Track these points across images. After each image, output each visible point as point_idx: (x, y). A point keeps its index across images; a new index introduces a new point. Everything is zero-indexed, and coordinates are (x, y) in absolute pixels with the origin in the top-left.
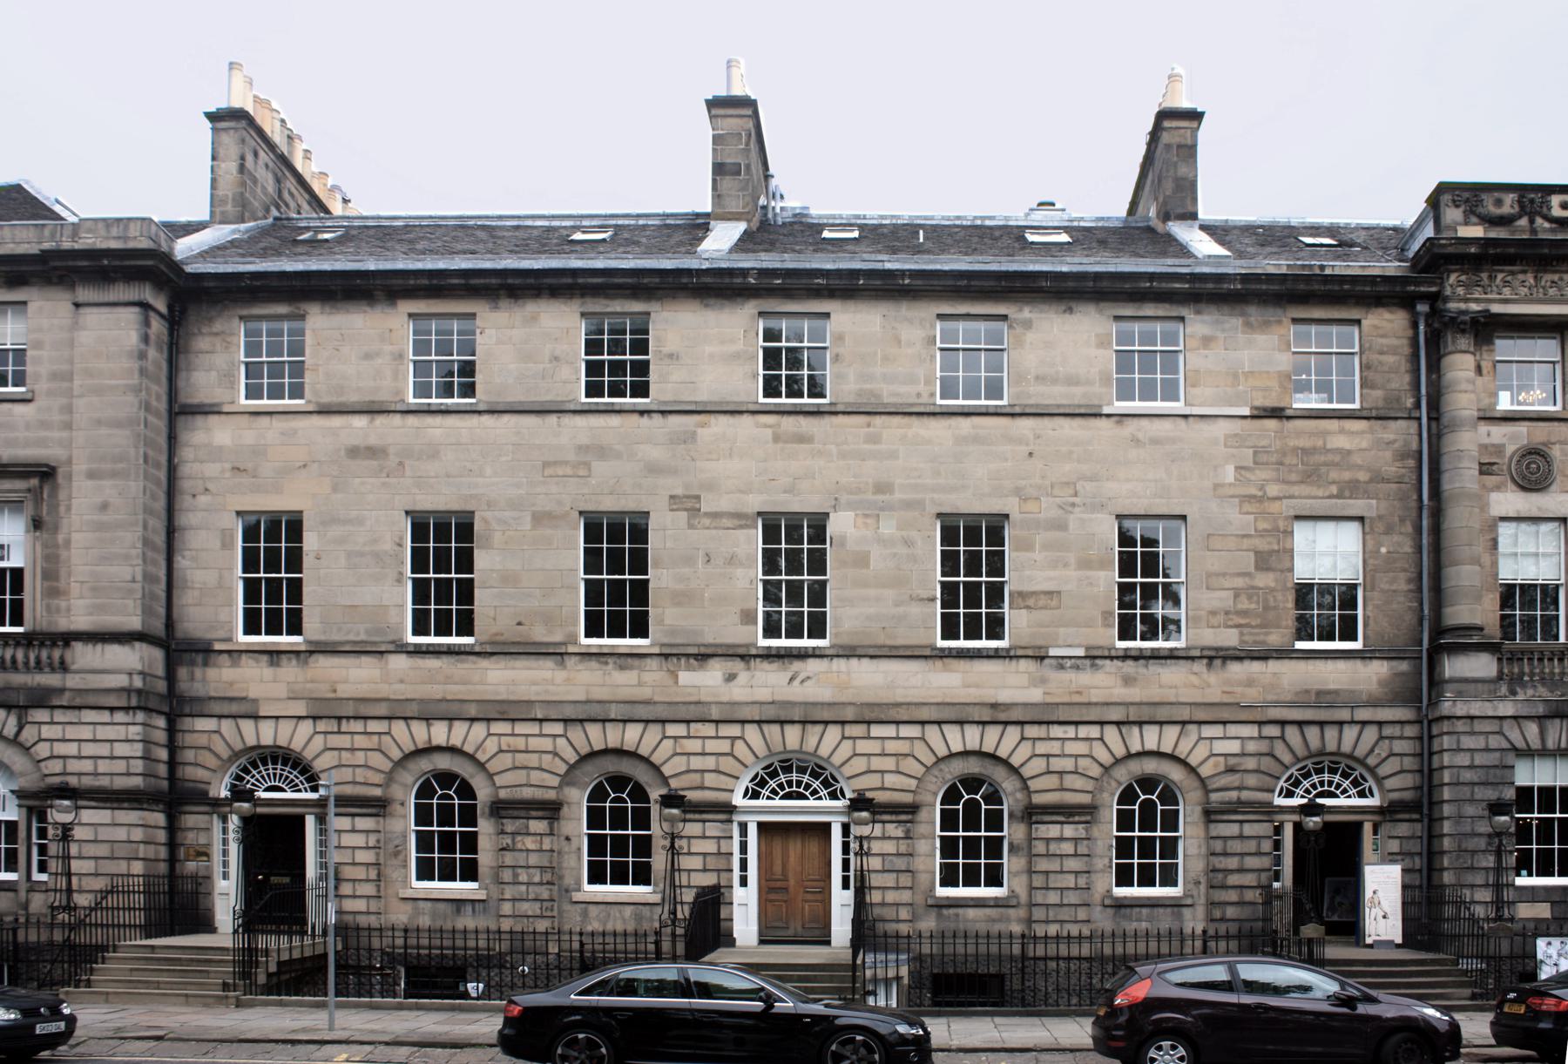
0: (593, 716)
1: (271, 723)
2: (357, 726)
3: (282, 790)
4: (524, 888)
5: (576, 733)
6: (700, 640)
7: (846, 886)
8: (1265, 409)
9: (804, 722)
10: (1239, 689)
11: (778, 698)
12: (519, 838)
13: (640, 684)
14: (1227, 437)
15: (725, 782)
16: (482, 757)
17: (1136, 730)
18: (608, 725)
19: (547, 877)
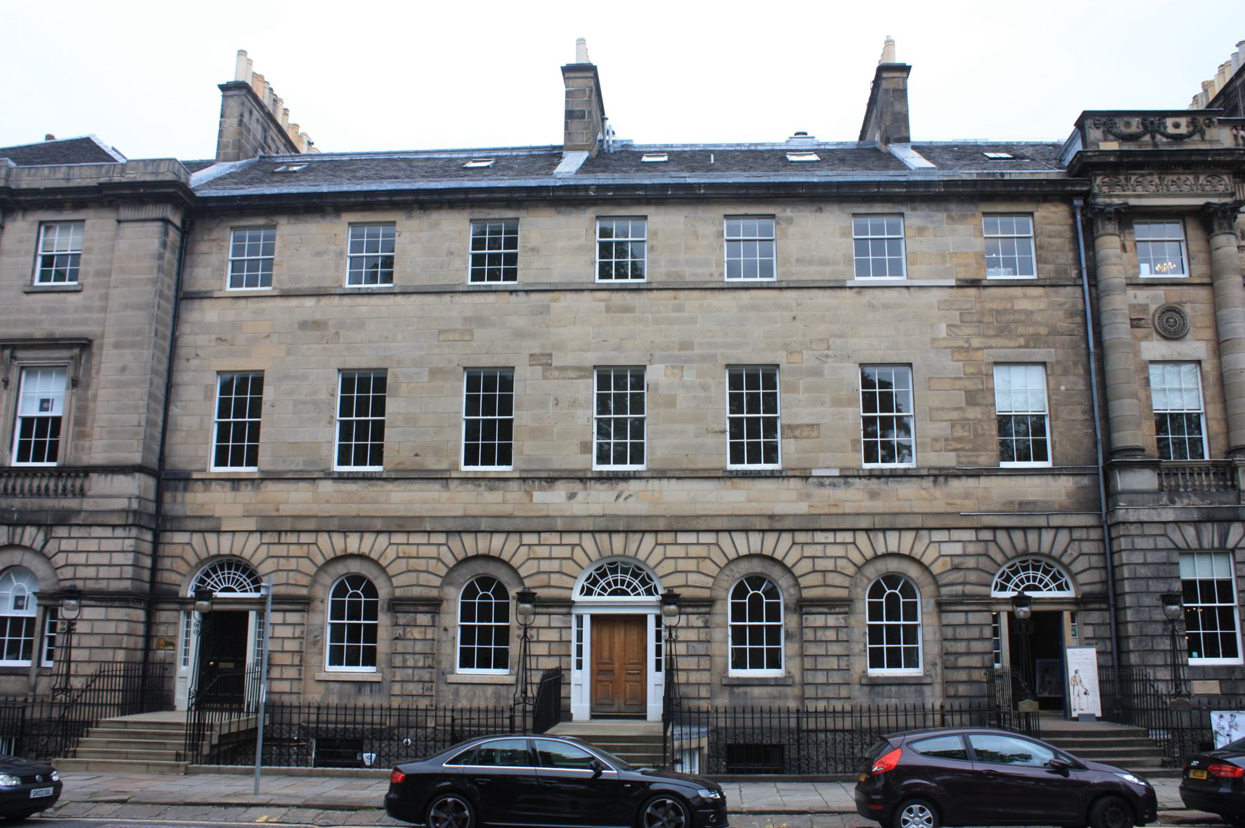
0: (468, 528)
1: (229, 536)
2: (292, 538)
3: (234, 591)
5: (455, 543)
6: (550, 467)
7: (658, 669)
8: (966, 281)
9: (626, 532)
10: (959, 501)
11: (607, 512)
13: (504, 502)
14: (939, 302)
15: (566, 581)
16: (383, 562)
17: (880, 535)
18: (479, 535)
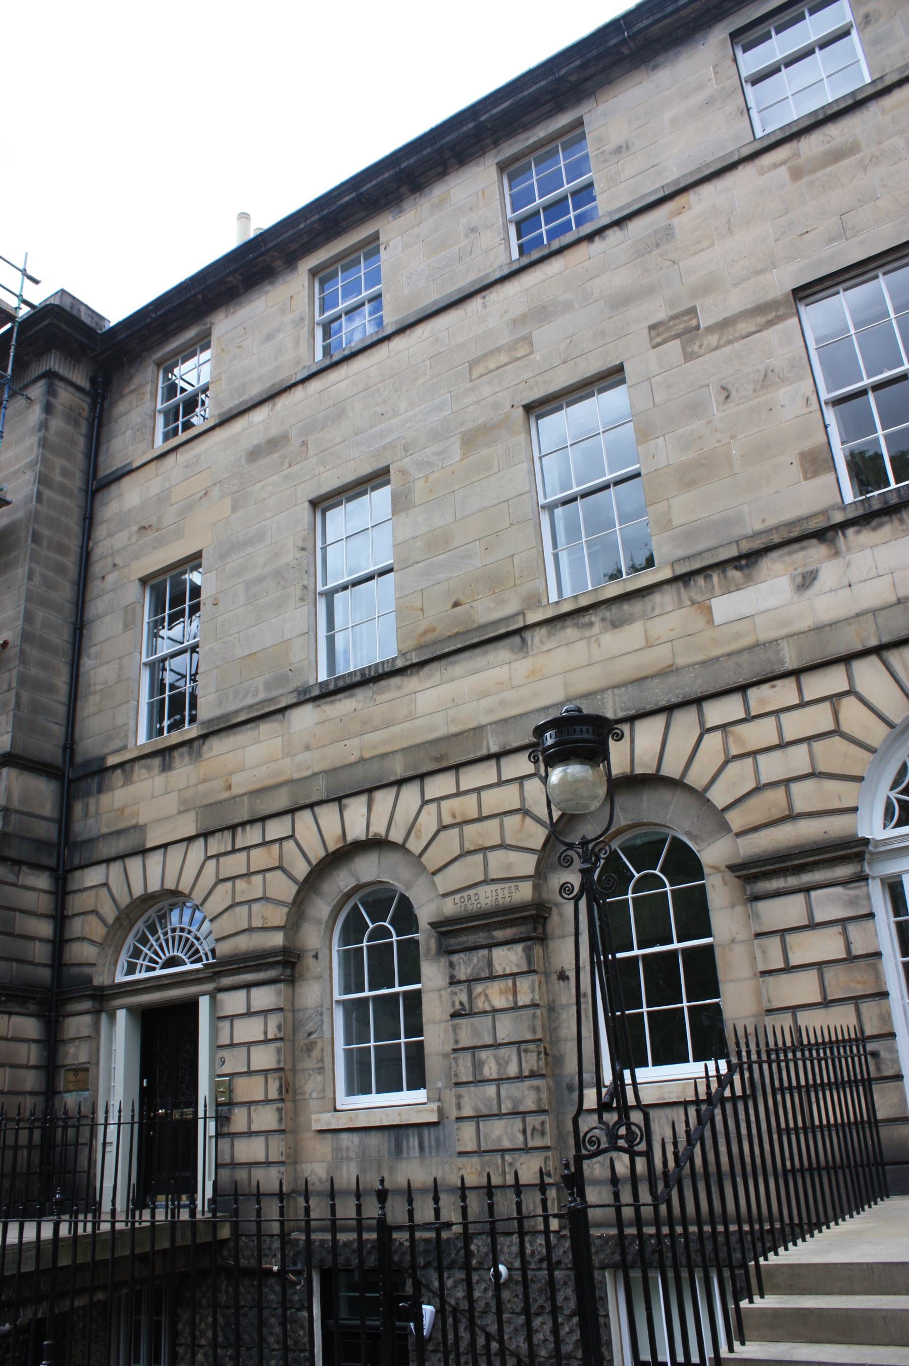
4: (491, 1090)
6: (738, 532)
12: (478, 988)
13: (649, 645)
15: (843, 794)
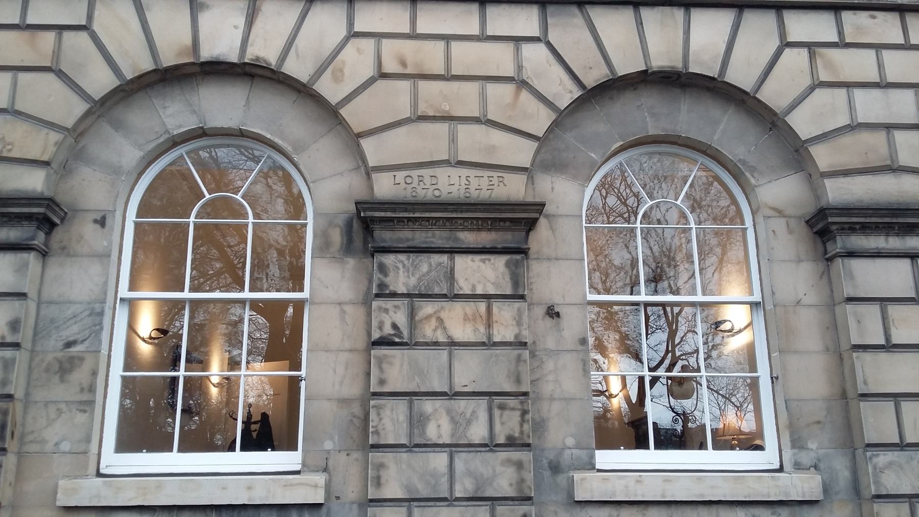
4: (440, 460)
12: (427, 308)
16: (330, 90)
19: (508, 424)
